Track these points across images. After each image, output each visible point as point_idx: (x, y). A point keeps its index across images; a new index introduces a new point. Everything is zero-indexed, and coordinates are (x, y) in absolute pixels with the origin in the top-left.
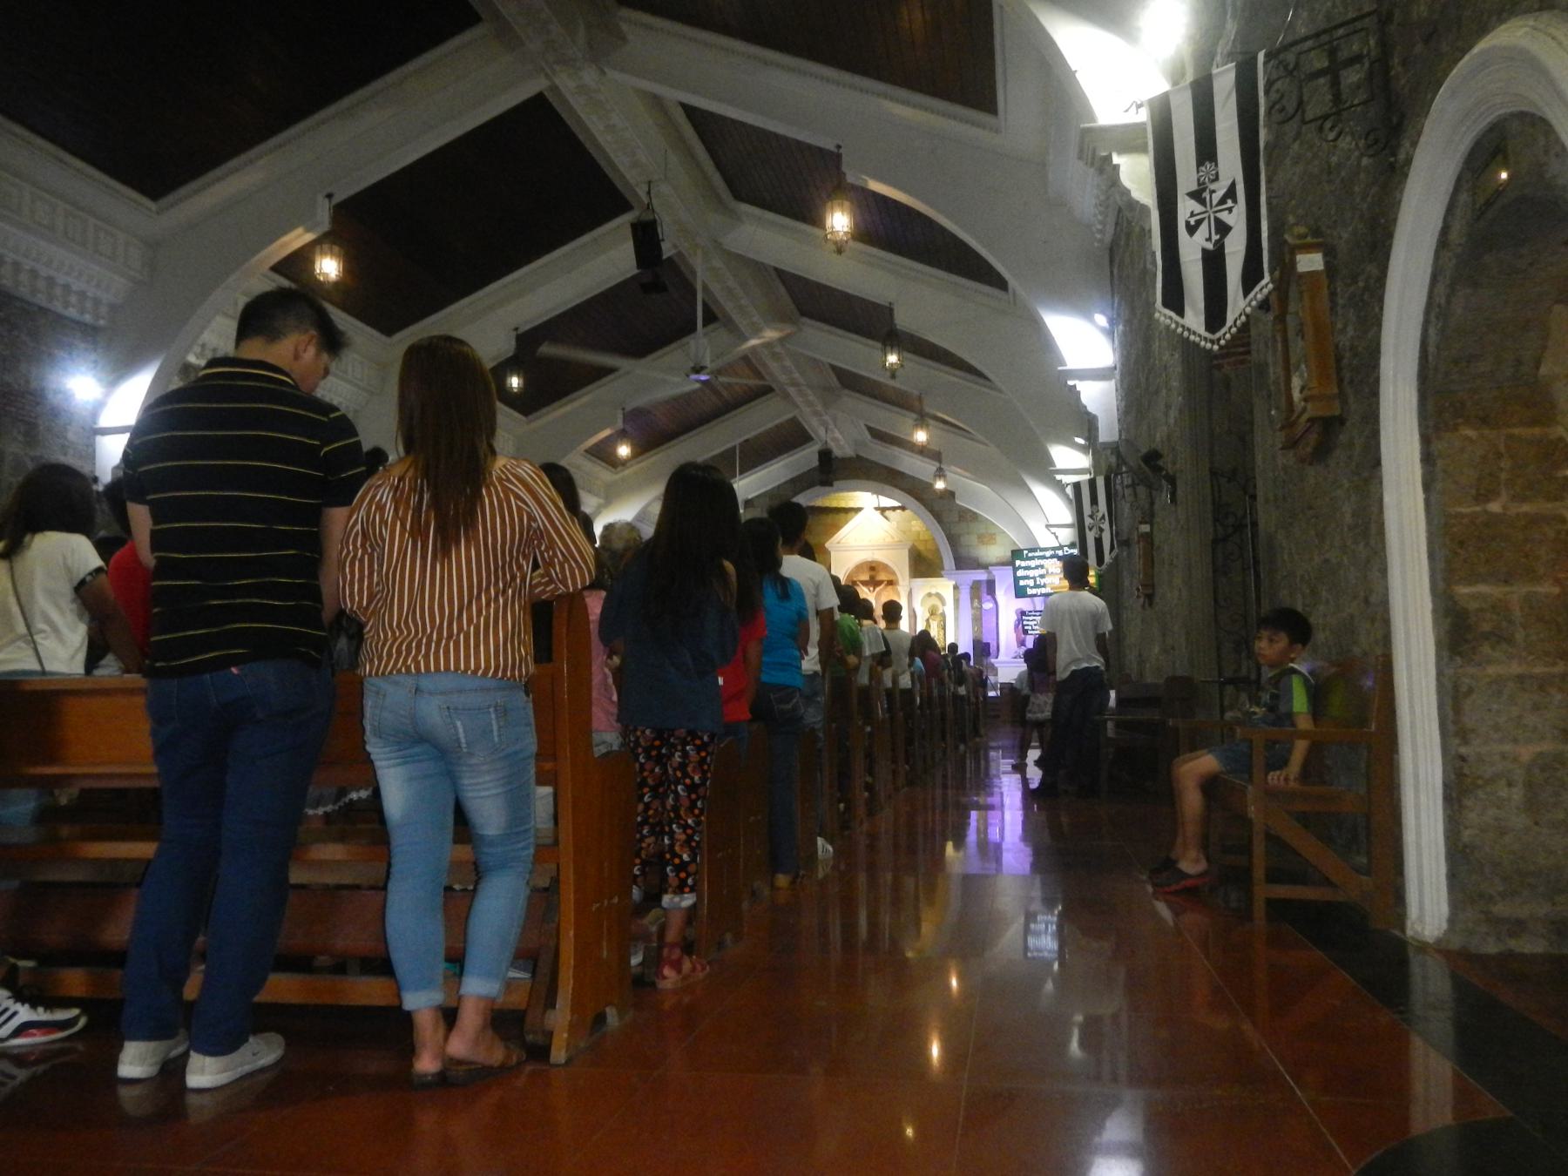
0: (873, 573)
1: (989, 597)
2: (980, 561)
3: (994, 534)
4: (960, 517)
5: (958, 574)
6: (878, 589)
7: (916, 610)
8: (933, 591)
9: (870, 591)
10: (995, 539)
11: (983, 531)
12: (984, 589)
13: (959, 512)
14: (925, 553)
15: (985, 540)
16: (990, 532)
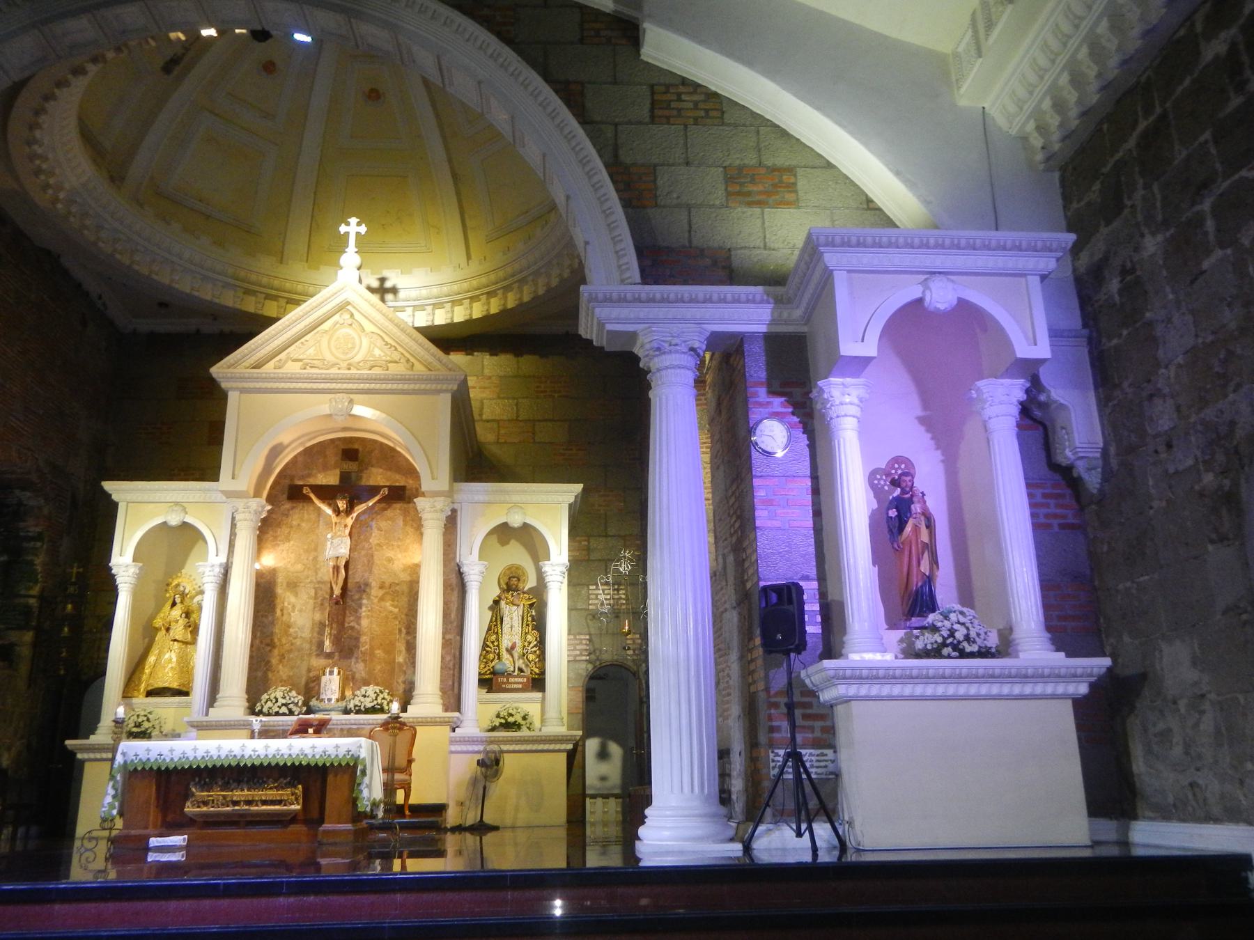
0: (351, 466)
1: (777, 403)
2: (736, 262)
3: (791, 170)
4: (653, 103)
5: (652, 300)
6: (360, 508)
7: (465, 569)
8: (516, 520)
9: (337, 512)
10: (792, 187)
11: (750, 159)
12: (756, 367)
13: (652, 87)
14: (495, 449)
15: (760, 188)
16: (769, 163)
